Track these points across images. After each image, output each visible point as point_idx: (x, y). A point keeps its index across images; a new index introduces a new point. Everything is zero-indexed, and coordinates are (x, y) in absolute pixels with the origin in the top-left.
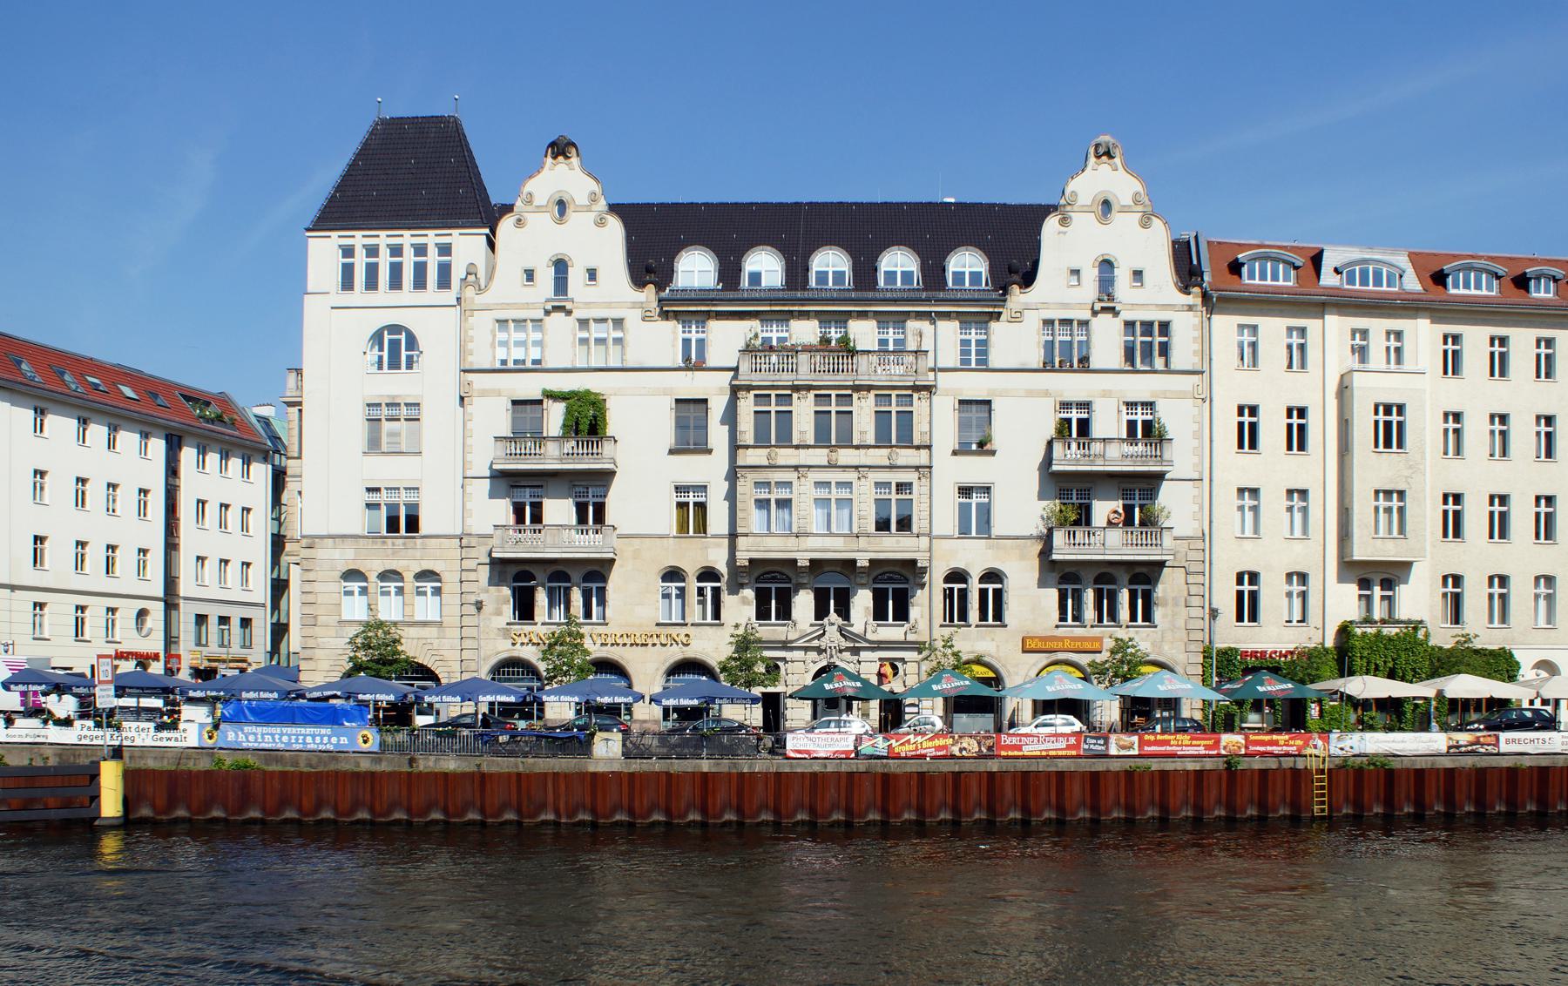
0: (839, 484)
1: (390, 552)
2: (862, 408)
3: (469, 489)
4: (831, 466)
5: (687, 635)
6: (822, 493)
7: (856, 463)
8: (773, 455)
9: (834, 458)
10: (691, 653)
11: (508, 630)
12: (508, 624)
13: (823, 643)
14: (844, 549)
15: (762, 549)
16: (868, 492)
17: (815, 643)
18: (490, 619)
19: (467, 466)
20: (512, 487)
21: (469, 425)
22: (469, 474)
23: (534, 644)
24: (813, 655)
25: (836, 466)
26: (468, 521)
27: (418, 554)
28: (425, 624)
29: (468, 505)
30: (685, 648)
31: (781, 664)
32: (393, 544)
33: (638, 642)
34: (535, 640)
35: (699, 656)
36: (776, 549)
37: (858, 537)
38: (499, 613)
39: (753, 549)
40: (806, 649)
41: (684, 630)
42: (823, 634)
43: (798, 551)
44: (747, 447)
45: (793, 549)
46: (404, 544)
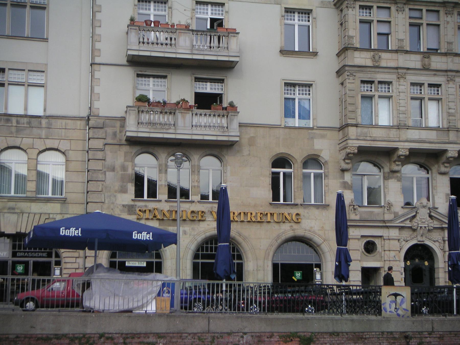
0: (430, 85)
1: (14, 129)
2: (448, 23)
3: (97, 75)
4: (426, 68)
5: (297, 214)
6: (415, 91)
7: (444, 67)
8: (377, 57)
9: (427, 63)
10: (300, 232)
11: (132, 206)
12: (132, 200)
13: (414, 224)
14: (436, 141)
15: (368, 138)
16: (455, 93)
17: (408, 224)
18: (115, 196)
19: (96, 53)
20: (138, 76)
21: (98, 16)
22: (97, 60)
23: (159, 219)
24: (406, 234)
25: (428, 69)
26: (96, 105)
27: (43, 133)
28: (48, 200)
29: (97, 90)
30: (295, 226)
31: (377, 241)
32: (18, 122)
33: (254, 219)
34: (159, 217)
35: (308, 235)
36: (380, 139)
37: (449, 130)
38: (124, 190)
39: (361, 138)
40: (401, 228)
41: (294, 211)
42: (414, 217)
43: (399, 141)
44: (356, 49)
45: (394, 139)
46: (29, 123)
